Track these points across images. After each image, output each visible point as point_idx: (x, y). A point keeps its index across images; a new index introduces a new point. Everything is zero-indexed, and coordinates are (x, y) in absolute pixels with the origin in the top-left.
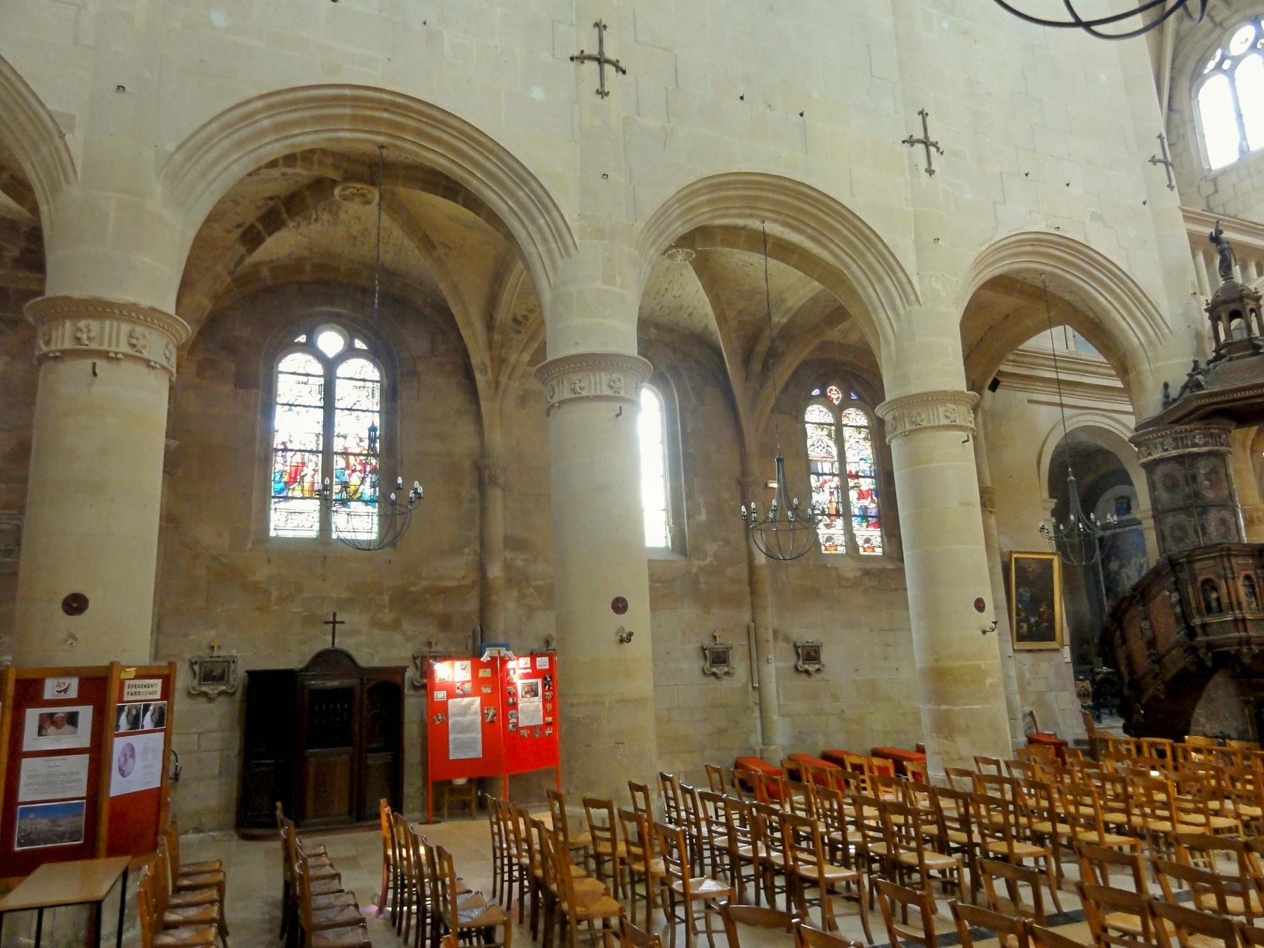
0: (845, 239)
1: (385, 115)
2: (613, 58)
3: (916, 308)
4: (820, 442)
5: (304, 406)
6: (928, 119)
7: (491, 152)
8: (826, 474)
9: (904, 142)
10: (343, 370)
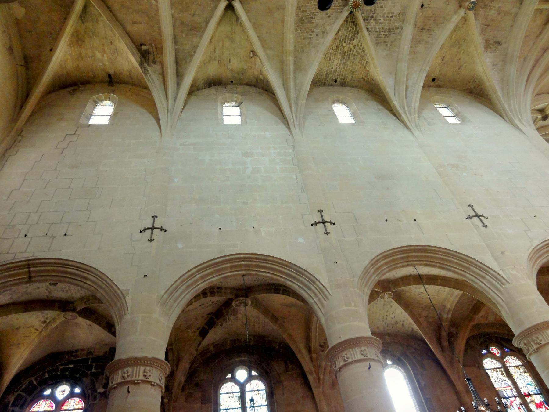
0: (456, 263)
1: (243, 263)
2: (329, 220)
3: (508, 285)
4: (498, 379)
5: (233, 409)
6: (474, 207)
7: (286, 266)
8: (510, 397)
9: (467, 219)
10: (248, 387)
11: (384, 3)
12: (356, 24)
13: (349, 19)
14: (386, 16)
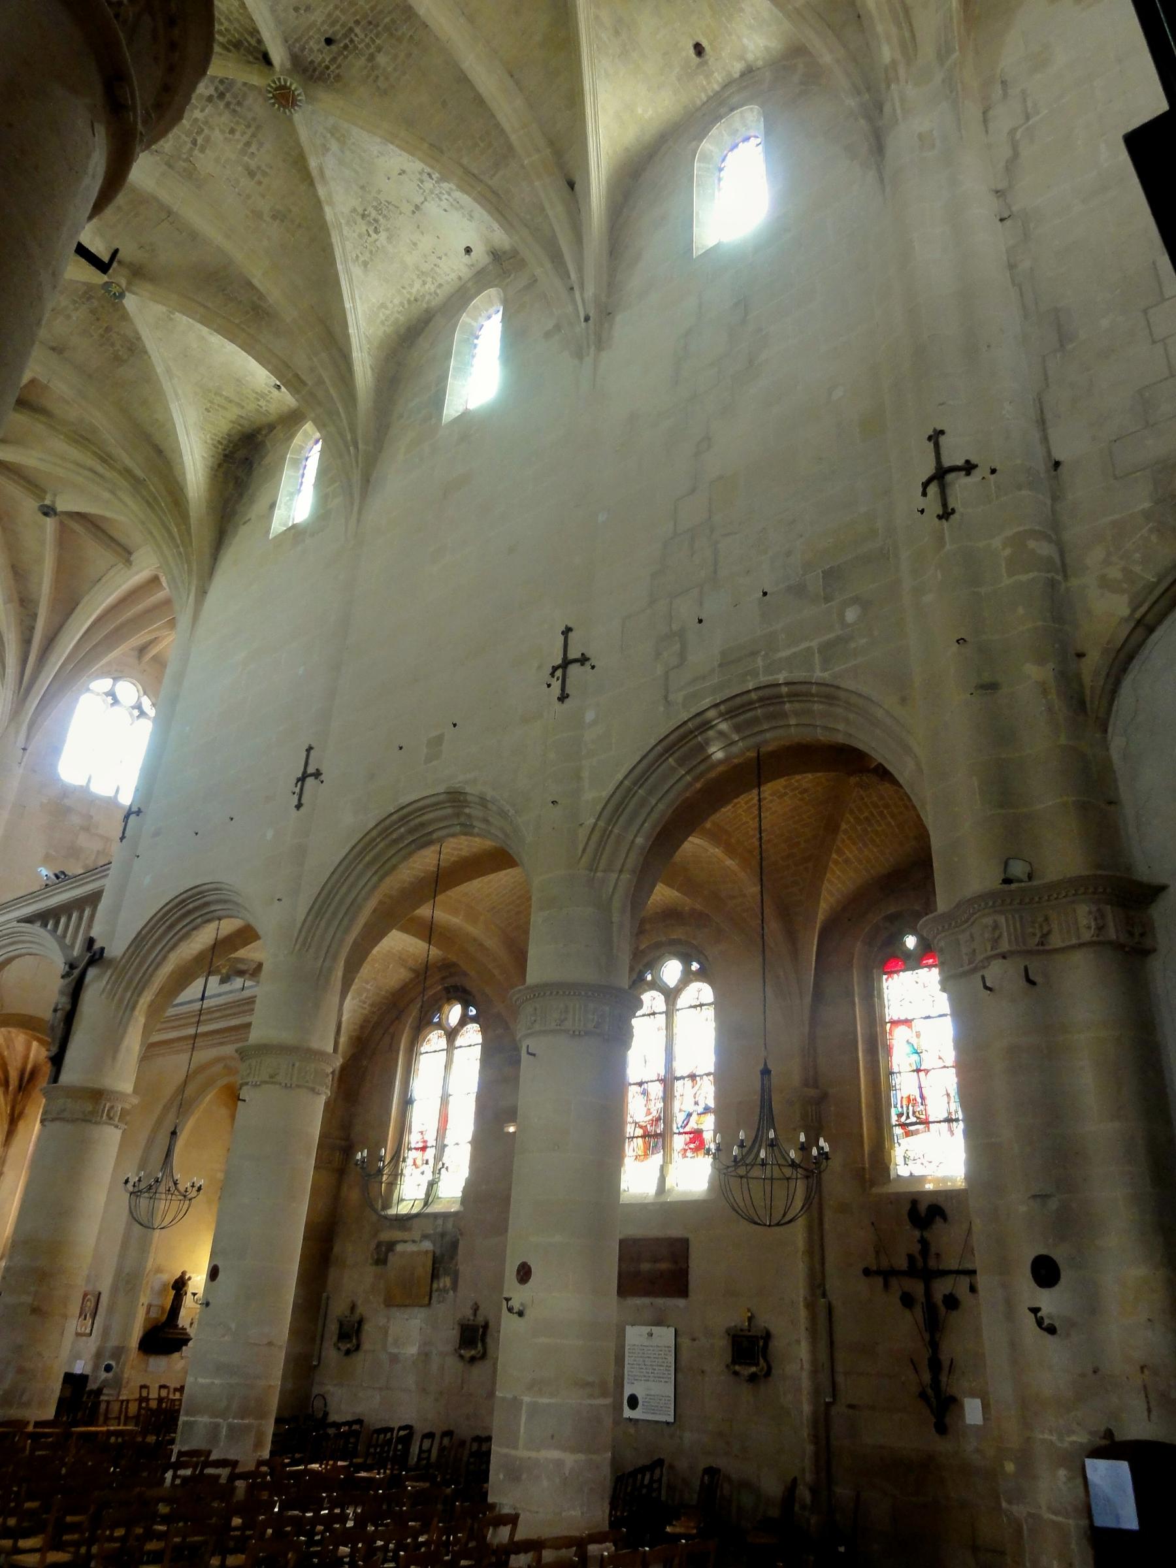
11: (238, 141)
12: (228, 50)
13: (253, 42)
14: (202, 130)
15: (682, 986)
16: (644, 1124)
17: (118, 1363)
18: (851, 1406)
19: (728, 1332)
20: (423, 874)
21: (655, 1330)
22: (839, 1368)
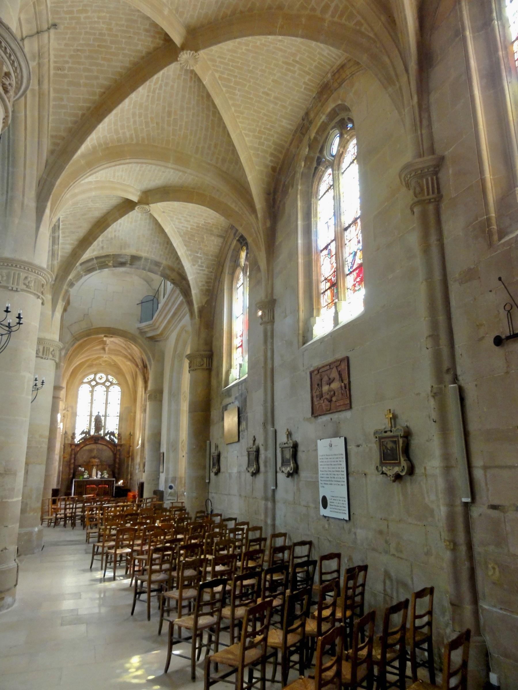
15: (342, 150)
16: (329, 278)
17: (175, 485)
18: (494, 507)
19: (376, 433)
20: (80, 113)
21: (334, 440)
22: (478, 462)
